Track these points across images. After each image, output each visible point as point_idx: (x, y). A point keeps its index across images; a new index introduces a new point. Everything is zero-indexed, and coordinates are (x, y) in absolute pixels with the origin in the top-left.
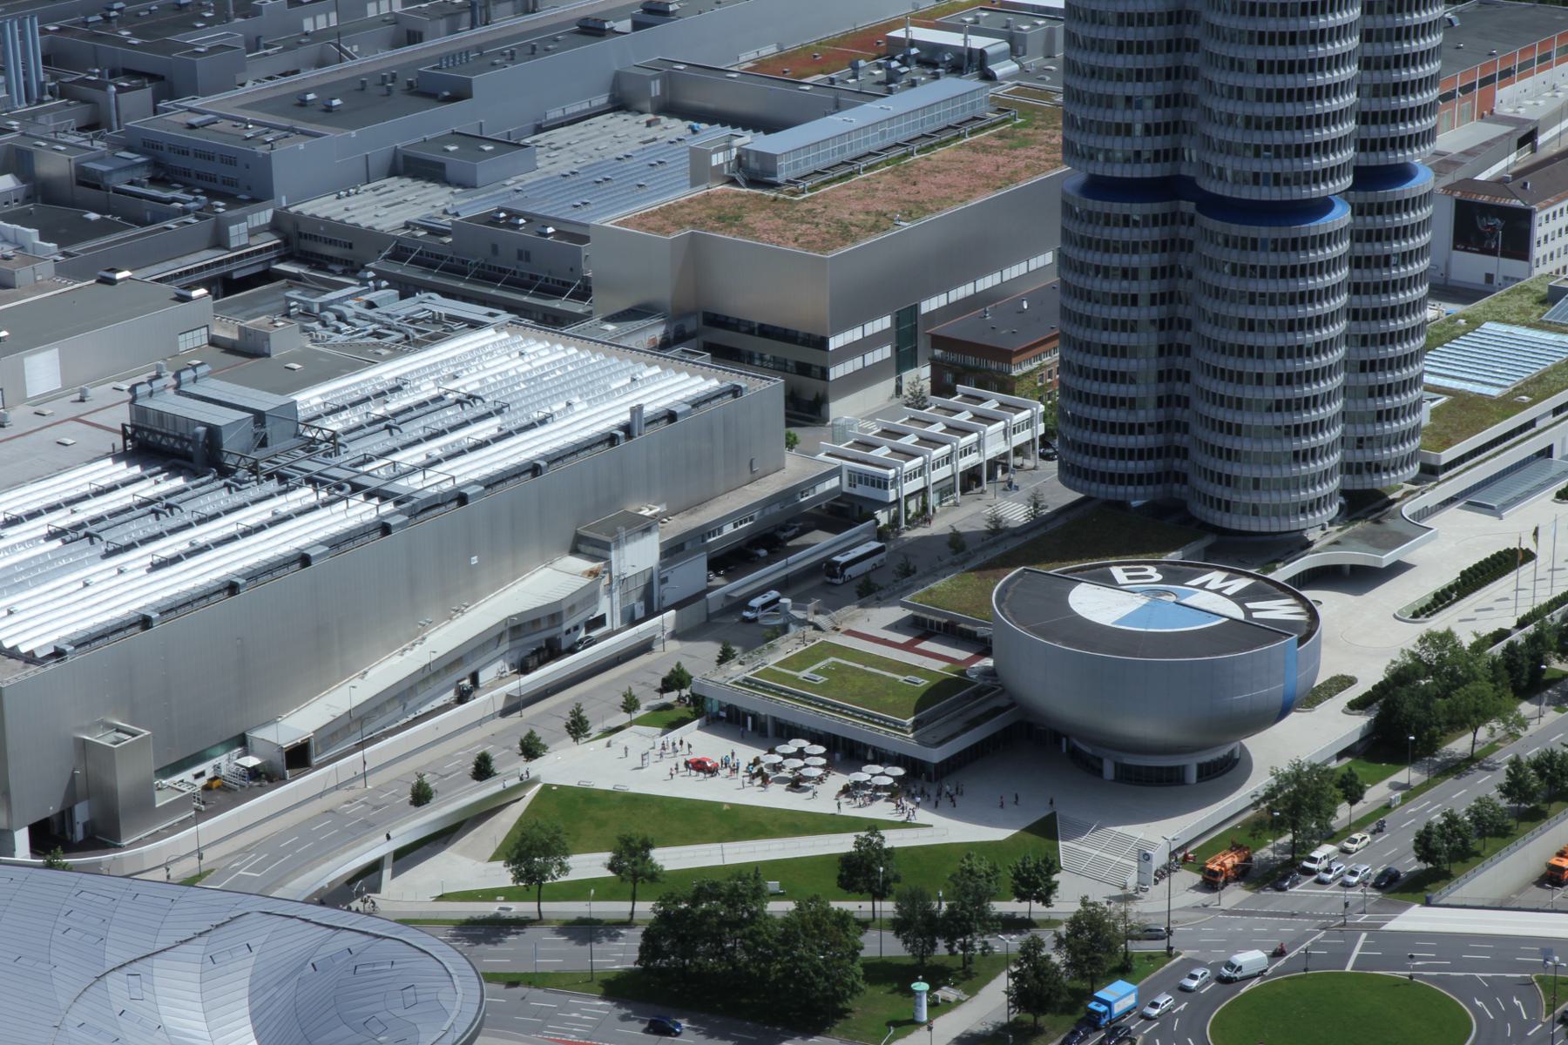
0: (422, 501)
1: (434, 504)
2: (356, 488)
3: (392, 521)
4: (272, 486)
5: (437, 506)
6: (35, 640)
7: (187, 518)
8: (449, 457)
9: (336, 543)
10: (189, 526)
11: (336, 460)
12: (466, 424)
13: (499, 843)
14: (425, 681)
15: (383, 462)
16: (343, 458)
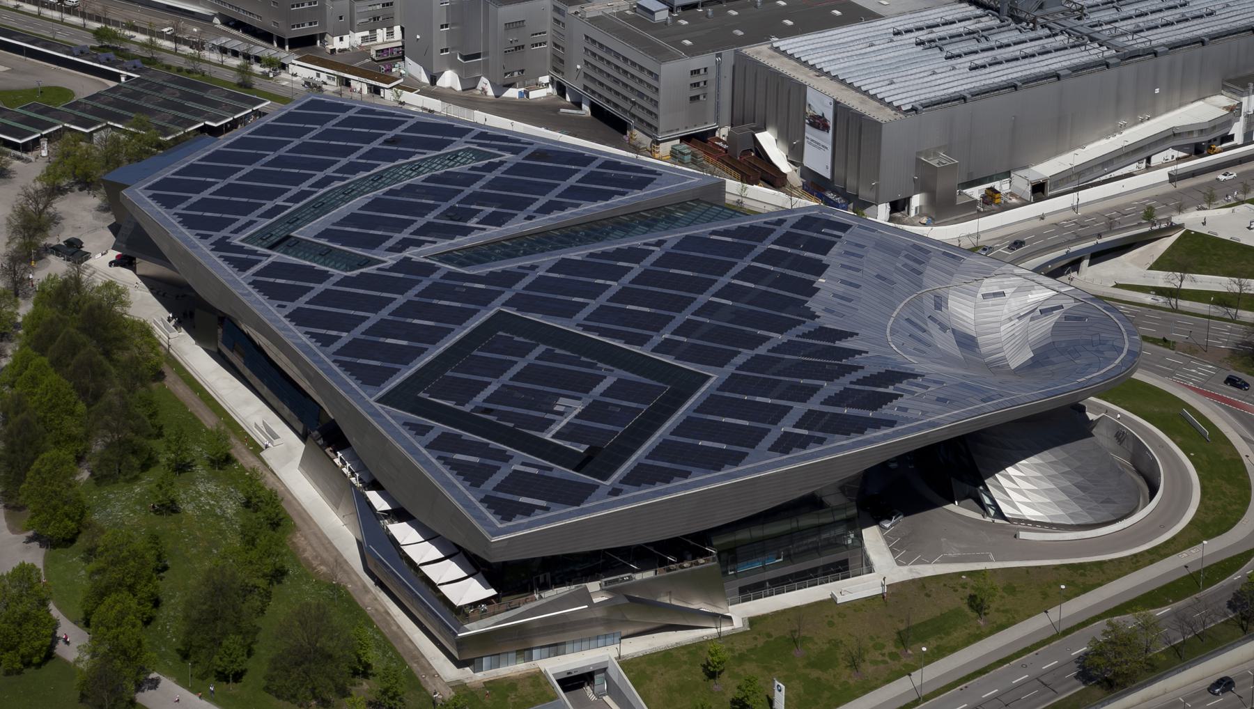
0: (1131, 52)
1: (1135, 55)
2: (1092, 40)
3: (1111, 61)
4: (1047, 31)
5: (1139, 56)
6: (906, 102)
7: (993, 44)
8: (1148, 29)
9: (1077, 70)
10: (992, 49)
11: (1081, 22)
12: (1160, 11)
13: (1155, 260)
14: (1119, 157)
15: (1109, 26)
16: (1085, 21)
